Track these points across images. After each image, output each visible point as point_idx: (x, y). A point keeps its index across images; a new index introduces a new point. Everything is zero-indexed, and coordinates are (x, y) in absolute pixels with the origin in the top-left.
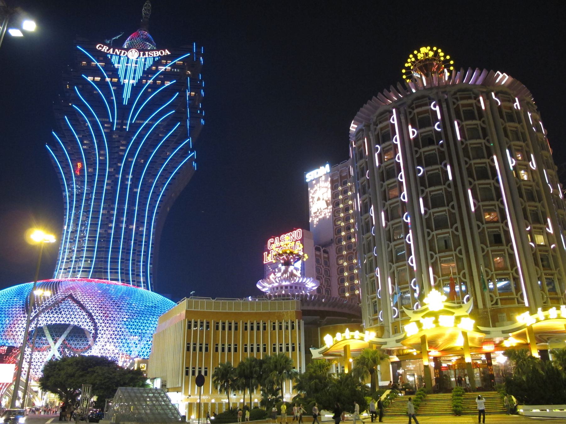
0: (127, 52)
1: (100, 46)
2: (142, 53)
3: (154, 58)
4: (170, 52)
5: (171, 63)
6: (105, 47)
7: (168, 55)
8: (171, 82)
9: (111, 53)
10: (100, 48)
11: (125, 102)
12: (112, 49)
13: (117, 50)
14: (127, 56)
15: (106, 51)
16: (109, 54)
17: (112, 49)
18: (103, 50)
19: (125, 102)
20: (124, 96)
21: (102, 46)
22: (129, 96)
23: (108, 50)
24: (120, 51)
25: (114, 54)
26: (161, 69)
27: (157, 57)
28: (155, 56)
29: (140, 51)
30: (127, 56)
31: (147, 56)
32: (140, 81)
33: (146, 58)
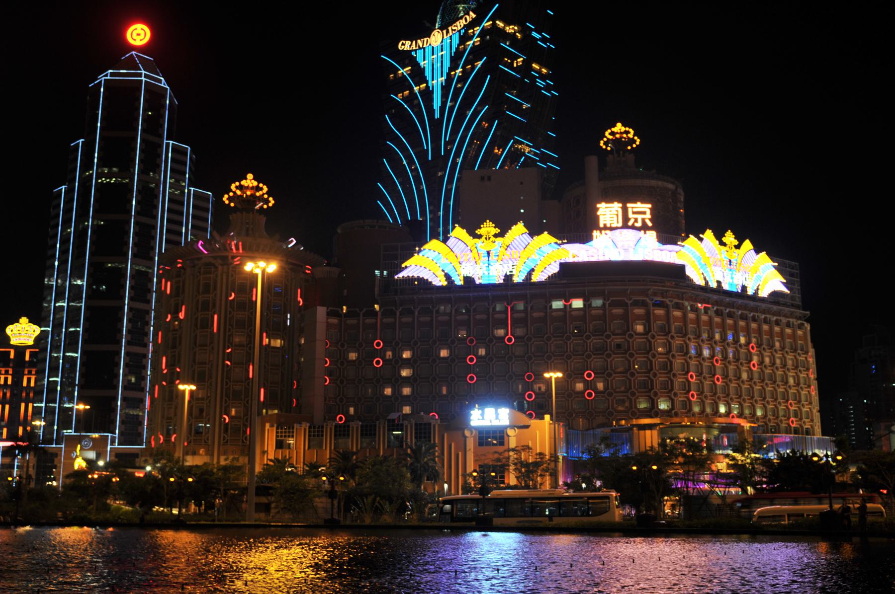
0: (429, 37)
1: (403, 44)
2: (445, 32)
3: (459, 31)
4: (475, 14)
5: (478, 30)
6: (407, 42)
7: (474, 20)
8: (481, 60)
9: (414, 48)
10: (403, 47)
11: (437, 115)
12: (414, 42)
13: (419, 41)
14: (430, 45)
15: (408, 49)
16: (412, 50)
17: (414, 42)
18: (405, 49)
19: (437, 115)
20: (435, 107)
21: (404, 42)
22: (439, 104)
23: (410, 46)
24: (422, 40)
25: (417, 48)
26: (469, 45)
27: (462, 29)
28: (459, 28)
29: (442, 31)
30: (430, 45)
31: (451, 34)
32: (448, 74)
33: (451, 37)
